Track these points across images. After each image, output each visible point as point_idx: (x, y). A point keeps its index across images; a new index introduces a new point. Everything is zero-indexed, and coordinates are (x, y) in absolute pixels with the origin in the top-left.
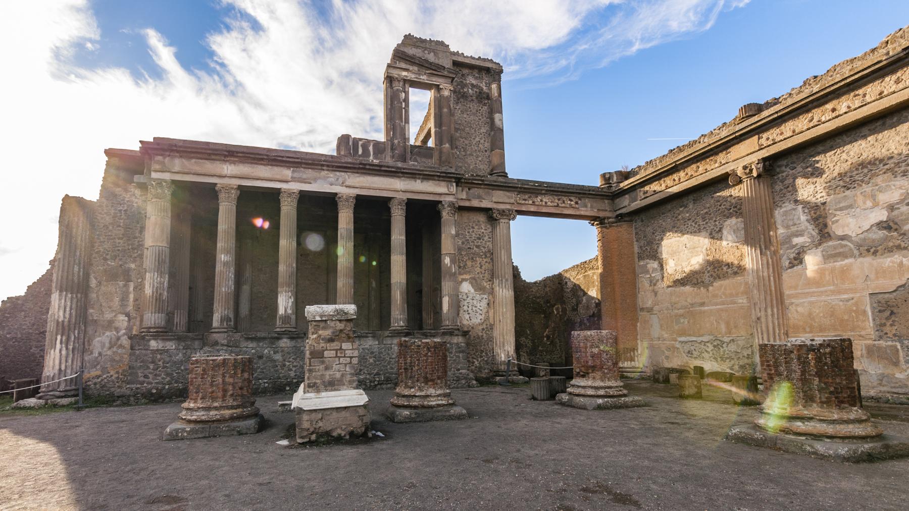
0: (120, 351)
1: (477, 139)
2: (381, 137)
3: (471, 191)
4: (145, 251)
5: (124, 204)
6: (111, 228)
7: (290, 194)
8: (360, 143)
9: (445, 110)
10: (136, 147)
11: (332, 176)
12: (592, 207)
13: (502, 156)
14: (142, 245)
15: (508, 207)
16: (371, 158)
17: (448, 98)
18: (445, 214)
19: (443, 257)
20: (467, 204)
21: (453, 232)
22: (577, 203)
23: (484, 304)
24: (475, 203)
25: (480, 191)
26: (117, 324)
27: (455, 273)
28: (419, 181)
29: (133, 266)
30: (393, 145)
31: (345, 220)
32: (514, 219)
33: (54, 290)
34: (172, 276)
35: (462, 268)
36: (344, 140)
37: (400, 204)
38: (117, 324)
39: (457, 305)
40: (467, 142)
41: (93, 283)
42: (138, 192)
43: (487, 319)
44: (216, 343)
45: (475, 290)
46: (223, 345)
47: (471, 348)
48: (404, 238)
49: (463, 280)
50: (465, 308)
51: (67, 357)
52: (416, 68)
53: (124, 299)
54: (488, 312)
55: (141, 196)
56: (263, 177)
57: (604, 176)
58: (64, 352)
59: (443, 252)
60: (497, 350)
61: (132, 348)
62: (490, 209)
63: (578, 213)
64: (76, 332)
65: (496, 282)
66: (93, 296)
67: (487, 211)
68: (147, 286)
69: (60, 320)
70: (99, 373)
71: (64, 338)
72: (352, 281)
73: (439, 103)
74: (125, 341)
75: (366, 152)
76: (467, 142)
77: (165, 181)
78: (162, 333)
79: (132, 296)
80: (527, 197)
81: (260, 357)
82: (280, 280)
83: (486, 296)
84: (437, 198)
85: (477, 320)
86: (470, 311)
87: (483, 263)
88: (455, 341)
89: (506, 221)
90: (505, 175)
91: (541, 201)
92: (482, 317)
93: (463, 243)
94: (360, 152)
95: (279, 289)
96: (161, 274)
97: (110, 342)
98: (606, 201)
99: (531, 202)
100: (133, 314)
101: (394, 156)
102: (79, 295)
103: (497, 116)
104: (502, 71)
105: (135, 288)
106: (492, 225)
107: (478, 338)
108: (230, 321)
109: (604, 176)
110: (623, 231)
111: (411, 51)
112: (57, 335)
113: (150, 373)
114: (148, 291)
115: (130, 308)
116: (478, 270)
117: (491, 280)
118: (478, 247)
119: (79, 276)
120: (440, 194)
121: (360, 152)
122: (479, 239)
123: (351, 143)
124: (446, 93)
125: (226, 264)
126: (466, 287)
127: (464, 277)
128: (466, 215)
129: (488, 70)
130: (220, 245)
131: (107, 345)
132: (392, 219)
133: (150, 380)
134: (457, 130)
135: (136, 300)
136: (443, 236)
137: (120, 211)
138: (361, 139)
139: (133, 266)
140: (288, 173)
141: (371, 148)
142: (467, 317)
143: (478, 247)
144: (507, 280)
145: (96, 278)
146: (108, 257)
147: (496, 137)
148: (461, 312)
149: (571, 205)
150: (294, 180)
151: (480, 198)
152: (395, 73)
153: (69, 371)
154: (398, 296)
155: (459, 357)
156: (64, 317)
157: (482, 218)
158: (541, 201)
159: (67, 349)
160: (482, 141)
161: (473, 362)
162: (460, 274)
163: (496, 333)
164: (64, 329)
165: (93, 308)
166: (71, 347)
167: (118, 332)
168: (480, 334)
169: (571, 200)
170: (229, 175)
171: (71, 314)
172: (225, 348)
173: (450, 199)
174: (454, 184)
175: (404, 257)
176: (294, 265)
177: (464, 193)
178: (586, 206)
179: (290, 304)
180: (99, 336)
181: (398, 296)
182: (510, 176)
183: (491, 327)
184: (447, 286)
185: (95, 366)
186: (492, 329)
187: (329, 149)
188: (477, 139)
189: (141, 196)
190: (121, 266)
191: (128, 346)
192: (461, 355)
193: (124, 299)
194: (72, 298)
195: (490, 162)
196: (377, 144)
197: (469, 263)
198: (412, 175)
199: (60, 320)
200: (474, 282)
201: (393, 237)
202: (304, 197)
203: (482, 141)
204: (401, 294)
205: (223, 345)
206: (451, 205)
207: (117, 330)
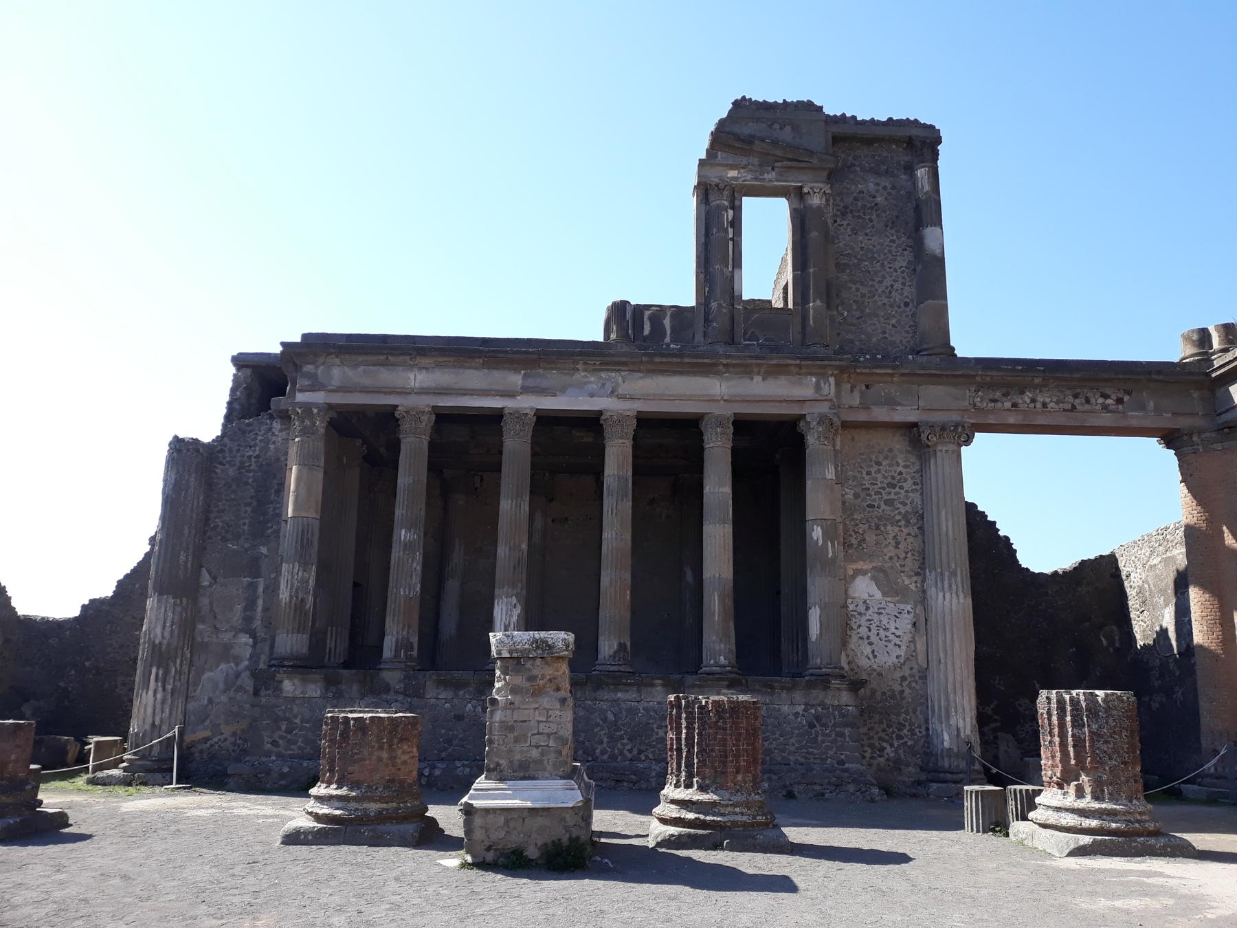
0: (239, 696)
1: (888, 282)
2: (686, 296)
3: (871, 390)
4: (283, 524)
5: (255, 445)
6: (234, 487)
7: (518, 415)
8: (647, 313)
9: (814, 234)
10: (278, 349)
12: (1158, 410)
13: (943, 312)
14: (279, 515)
15: (955, 417)
16: (668, 340)
18: (811, 440)
19: (808, 525)
20: (862, 417)
21: (830, 474)
22: (1120, 401)
23: (905, 623)
24: (881, 414)
26: (236, 651)
27: (834, 558)
28: (758, 379)
29: (264, 550)
30: (707, 314)
31: (617, 460)
32: (968, 441)
33: (150, 590)
34: (325, 568)
35: (852, 546)
36: (619, 312)
37: (720, 424)
38: (236, 651)
39: (843, 623)
40: (864, 290)
41: (206, 580)
42: (277, 425)
43: (912, 656)
44: (387, 688)
45: (884, 594)
46: (397, 692)
47: (877, 717)
48: (727, 490)
49: (857, 573)
50: (863, 631)
51: (163, 702)
52: (756, 161)
53: (250, 605)
54: (913, 641)
55: (281, 430)
58: (159, 696)
59: (810, 516)
60: (935, 725)
61: (256, 693)
62: (915, 425)
63: (1123, 423)
64: (178, 661)
65: (931, 577)
66: (204, 601)
67: (910, 429)
68: (283, 586)
69: (157, 642)
70: (207, 734)
71: (161, 672)
72: (627, 576)
74: (247, 682)
76: (864, 290)
77: (317, 405)
78: (302, 666)
79: (260, 602)
80: (998, 394)
81: (459, 718)
82: (499, 574)
83: (909, 608)
84: (795, 410)
85: (888, 658)
86: (874, 639)
87: (904, 535)
88: (836, 703)
89: (951, 447)
91: (1033, 401)
92: (902, 652)
93: (856, 496)
94: (647, 331)
95: (497, 591)
96: (305, 566)
97: (226, 682)
98: (1196, 395)
99: (1008, 405)
100: (261, 634)
102: (185, 600)
103: (929, 232)
104: (939, 140)
105: (266, 588)
106: (920, 457)
107: (893, 696)
108: (412, 649)
112: (151, 666)
113: (281, 737)
114: (284, 595)
115: (257, 623)
116: (890, 551)
117: (920, 572)
118: (887, 502)
119: (186, 566)
120: (802, 402)
121: (647, 331)
122: (894, 486)
123: (629, 316)
124: (816, 201)
125: (408, 546)
126: (864, 588)
127: (860, 565)
128: (863, 437)
129: (910, 142)
130: (399, 512)
131: (221, 686)
132: (706, 453)
133: (281, 750)
134: (841, 267)
135: (265, 610)
136: (809, 483)
137: (249, 457)
138: (648, 307)
139: (264, 550)
140: (516, 379)
141: (667, 322)
142: (868, 650)
143: (887, 502)
144: (954, 574)
145: (210, 573)
146: (229, 536)
147: (929, 275)
148: (854, 638)
149: (1105, 408)
150: (526, 390)
151: (891, 403)
152: (714, 175)
153: (164, 728)
154: (716, 605)
155: (842, 735)
156: (163, 637)
157: (898, 443)
158: (1033, 401)
159: (164, 689)
160: (898, 285)
161: (882, 749)
162: (849, 559)
163: (933, 688)
164: (161, 657)
165: (203, 622)
166: (169, 687)
167: (237, 665)
168: (897, 688)
169: (1106, 396)
171: (172, 631)
172: (400, 698)
173: (824, 408)
174: (832, 380)
175: (729, 529)
176: (524, 546)
177: (857, 394)
178: (1142, 407)
179: (514, 619)
180: (211, 670)
181: (716, 605)
182: (960, 353)
183: (924, 675)
184: (818, 587)
185: (203, 721)
186: (924, 678)
188: (888, 282)
189: (281, 430)
190: (247, 550)
191: (250, 689)
192: (847, 731)
193: (250, 605)
194: (175, 604)
195: (915, 325)
196: (678, 311)
197: (871, 538)
199: (157, 642)
200: (884, 579)
201: (706, 490)
202: (545, 420)
203: (898, 285)
204: (722, 601)
205: (397, 692)
207: (237, 660)
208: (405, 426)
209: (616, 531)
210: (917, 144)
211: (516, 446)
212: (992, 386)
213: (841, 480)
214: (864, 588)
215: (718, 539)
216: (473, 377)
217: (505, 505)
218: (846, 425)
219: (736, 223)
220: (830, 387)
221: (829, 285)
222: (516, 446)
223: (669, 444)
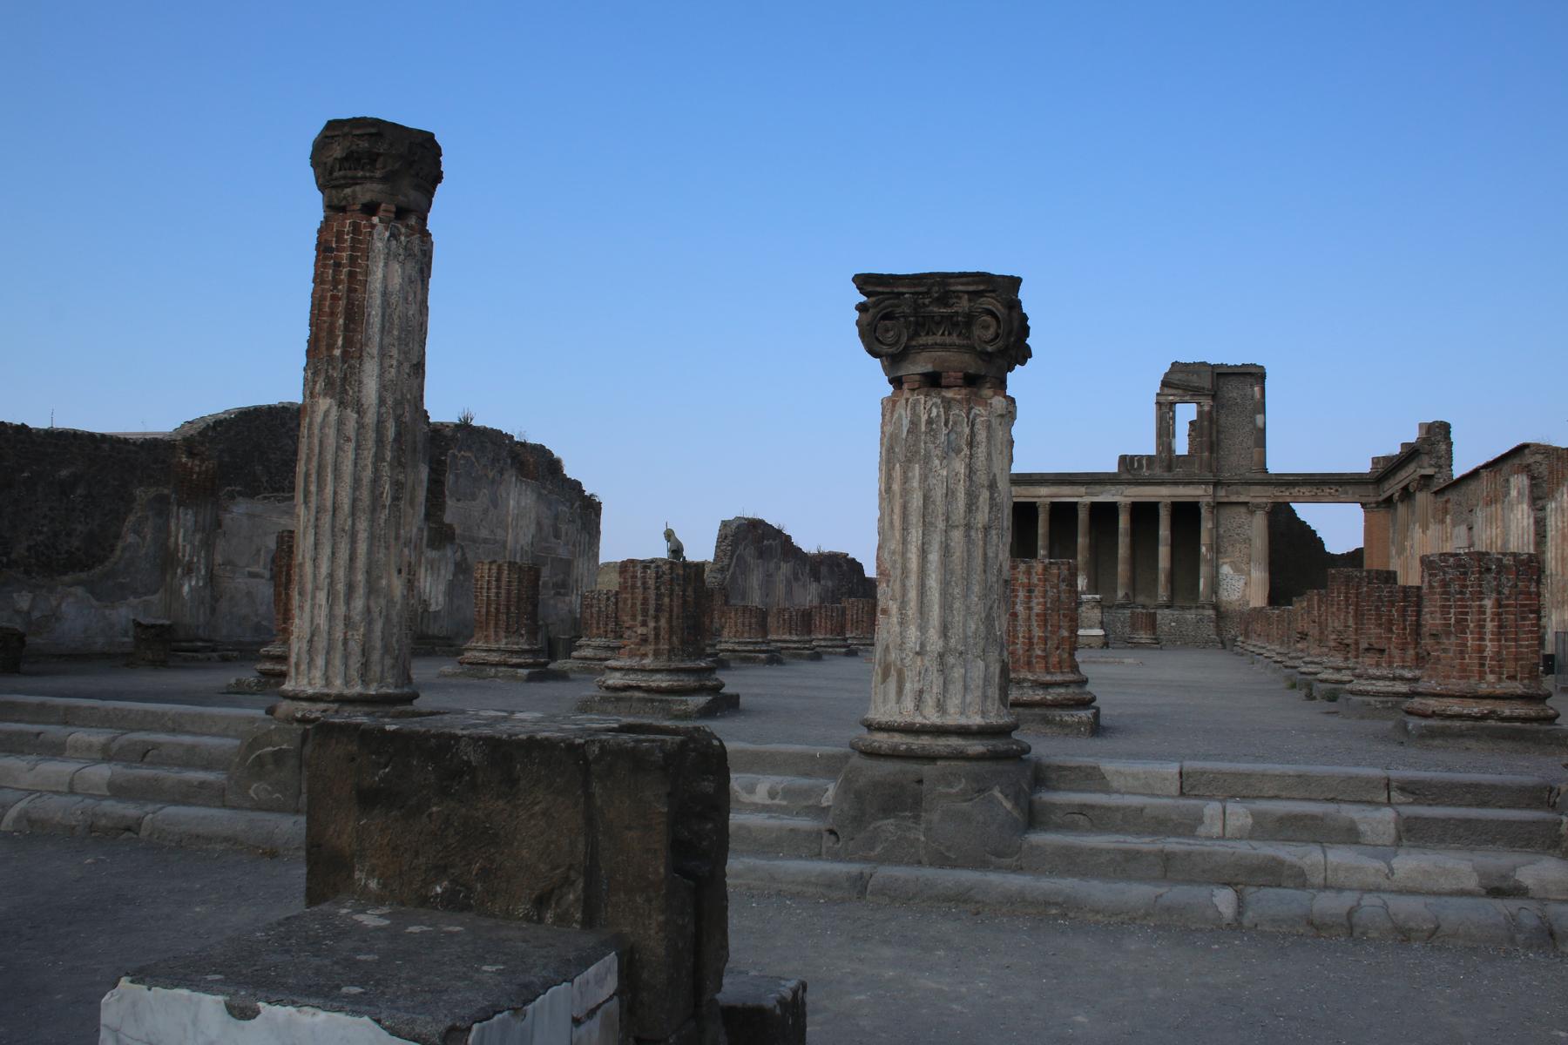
2: (1153, 452)
11: (1113, 489)
17: (1210, 412)
18: (1204, 512)
23: (1242, 583)
24: (1234, 499)
25: (1240, 488)
31: (1124, 521)
56: (1066, 494)
57: (1376, 461)
73: (1200, 413)
75: (1140, 465)
85: (1235, 597)
90: (1265, 470)
101: (1165, 463)
103: (1259, 418)
109: (1376, 461)
110: (1381, 515)
111: (1176, 378)
129: (1250, 374)
140: (1082, 490)
147: (1260, 437)
150: (1087, 494)
151: (1238, 493)
152: (1162, 399)
157: (1243, 510)
170: (1044, 495)
173: (1208, 499)
184: (1204, 570)
187: (1112, 467)
196: (1149, 457)
198: (1176, 483)
206: (1208, 504)
208: (1040, 510)
209: (1123, 550)
210: (1254, 375)
211: (1083, 516)
212: (1282, 484)
213: (1217, 526)
214: (1226, 569)
215: (1164, 552)
216: (1066, 490)
217: (1080, 540)
218: (1220, 504)
219: (1173, 418)
220: (1210, 489)
221: (1212, 443)
222: (1083, 516)
223: (1144, 513)
